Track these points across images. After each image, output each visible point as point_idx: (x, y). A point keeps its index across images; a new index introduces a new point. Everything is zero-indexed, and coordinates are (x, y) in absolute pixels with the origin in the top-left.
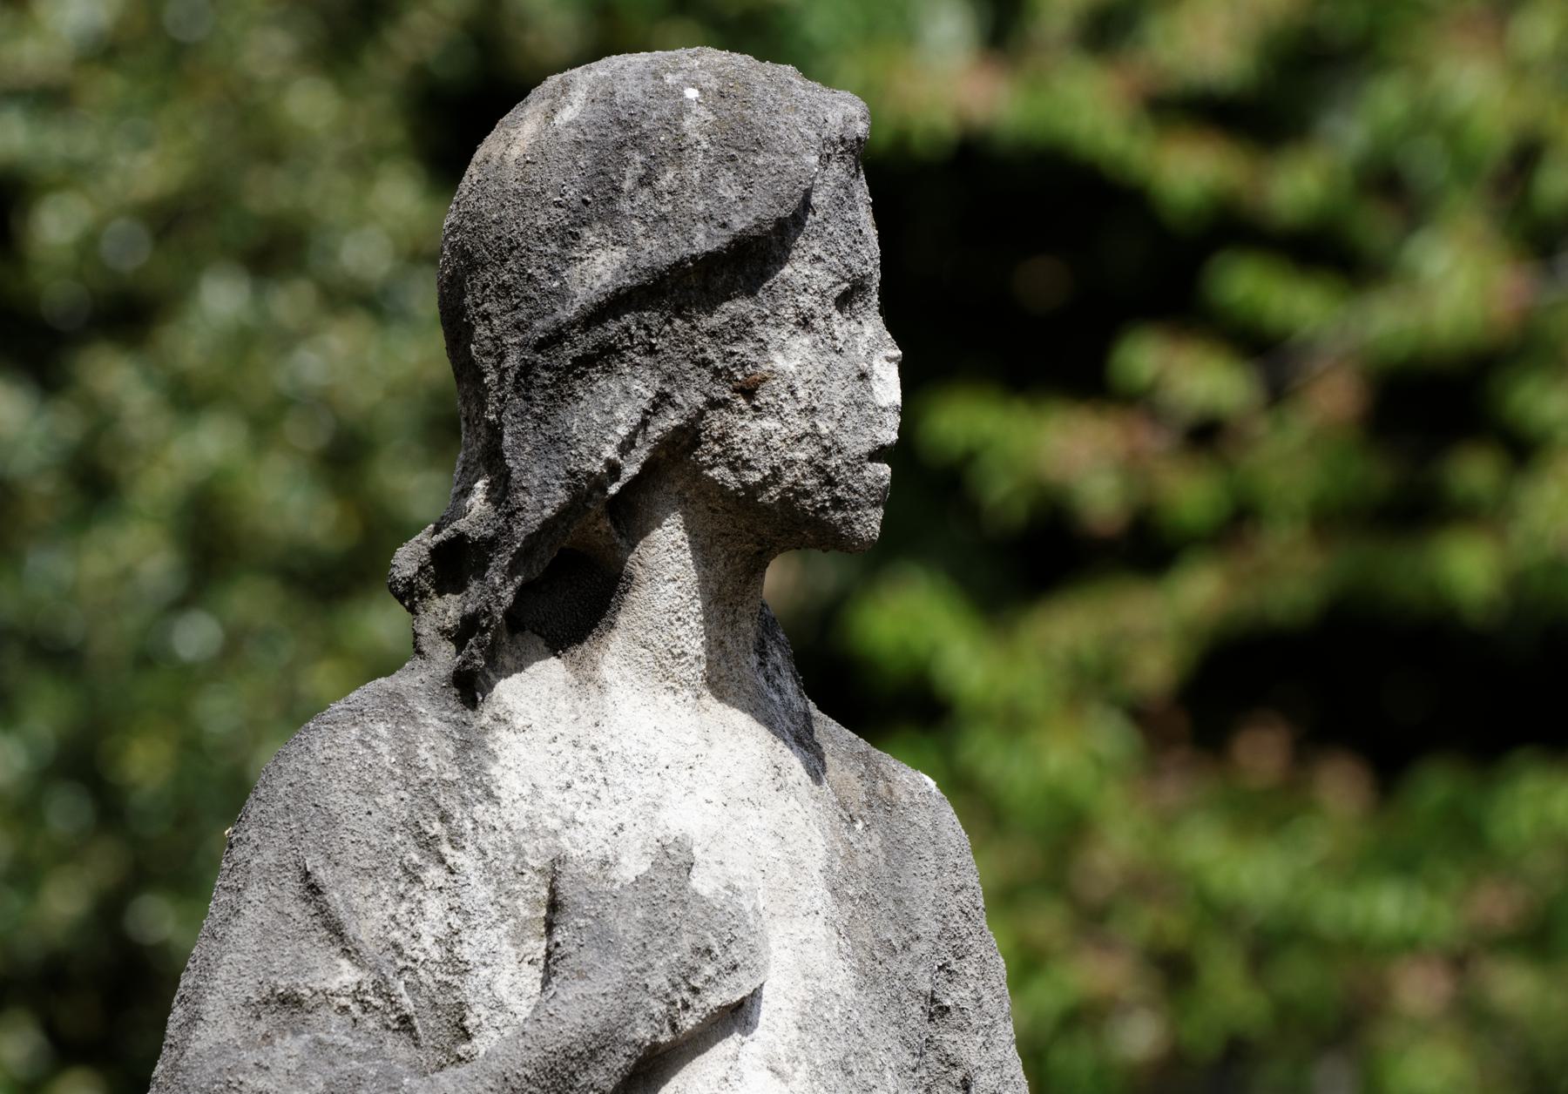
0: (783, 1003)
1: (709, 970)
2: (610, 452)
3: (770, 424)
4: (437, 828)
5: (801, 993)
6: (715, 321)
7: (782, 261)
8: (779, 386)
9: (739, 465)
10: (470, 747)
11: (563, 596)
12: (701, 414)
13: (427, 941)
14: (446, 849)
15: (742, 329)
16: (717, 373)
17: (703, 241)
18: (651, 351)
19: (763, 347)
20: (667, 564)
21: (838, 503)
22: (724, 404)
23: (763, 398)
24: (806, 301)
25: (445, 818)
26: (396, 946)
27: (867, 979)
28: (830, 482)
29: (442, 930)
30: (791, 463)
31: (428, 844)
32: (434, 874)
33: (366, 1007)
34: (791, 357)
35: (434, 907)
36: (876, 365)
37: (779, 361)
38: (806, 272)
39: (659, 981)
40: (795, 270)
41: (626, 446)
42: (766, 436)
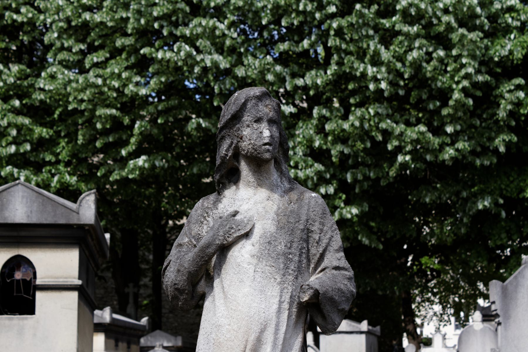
0: (258, 234)
1: (233, 231)
2: (224, 152)
3: (245, 143)
4: (206, 215)
5: (262, 232)
6: (235, 129)
7: (243, 117)
8: (244, 137)
9: (244, 150)
10: (218, 201)
11: (232, 176)
12: (237, 144)
13: (204, 233)
14: (207, 218)
15: (239, 129)
16: (237, 137)
17: (229, 117)
18: (229, 135)
19: (242, 132)
20: (244, 167)
21: (259, 153)
22: (239, 142)
23: (243, 139)
24: (247, 123)
25: (207, 213)
26: (199, 234)
27: (280, 228)
28: (256, 150)
29: (206, 231)
30: (249, 149)
31: (205, 217)
32: (205, 222)
33: (190, 244)
34: (246, 132)
35: (205, 227)
36: (264, 130)
37: (244, 133)
38: (247, 118)
39: (221, 233)
40: (245, 118)
41: (228, 150)
42: (245, 145)
